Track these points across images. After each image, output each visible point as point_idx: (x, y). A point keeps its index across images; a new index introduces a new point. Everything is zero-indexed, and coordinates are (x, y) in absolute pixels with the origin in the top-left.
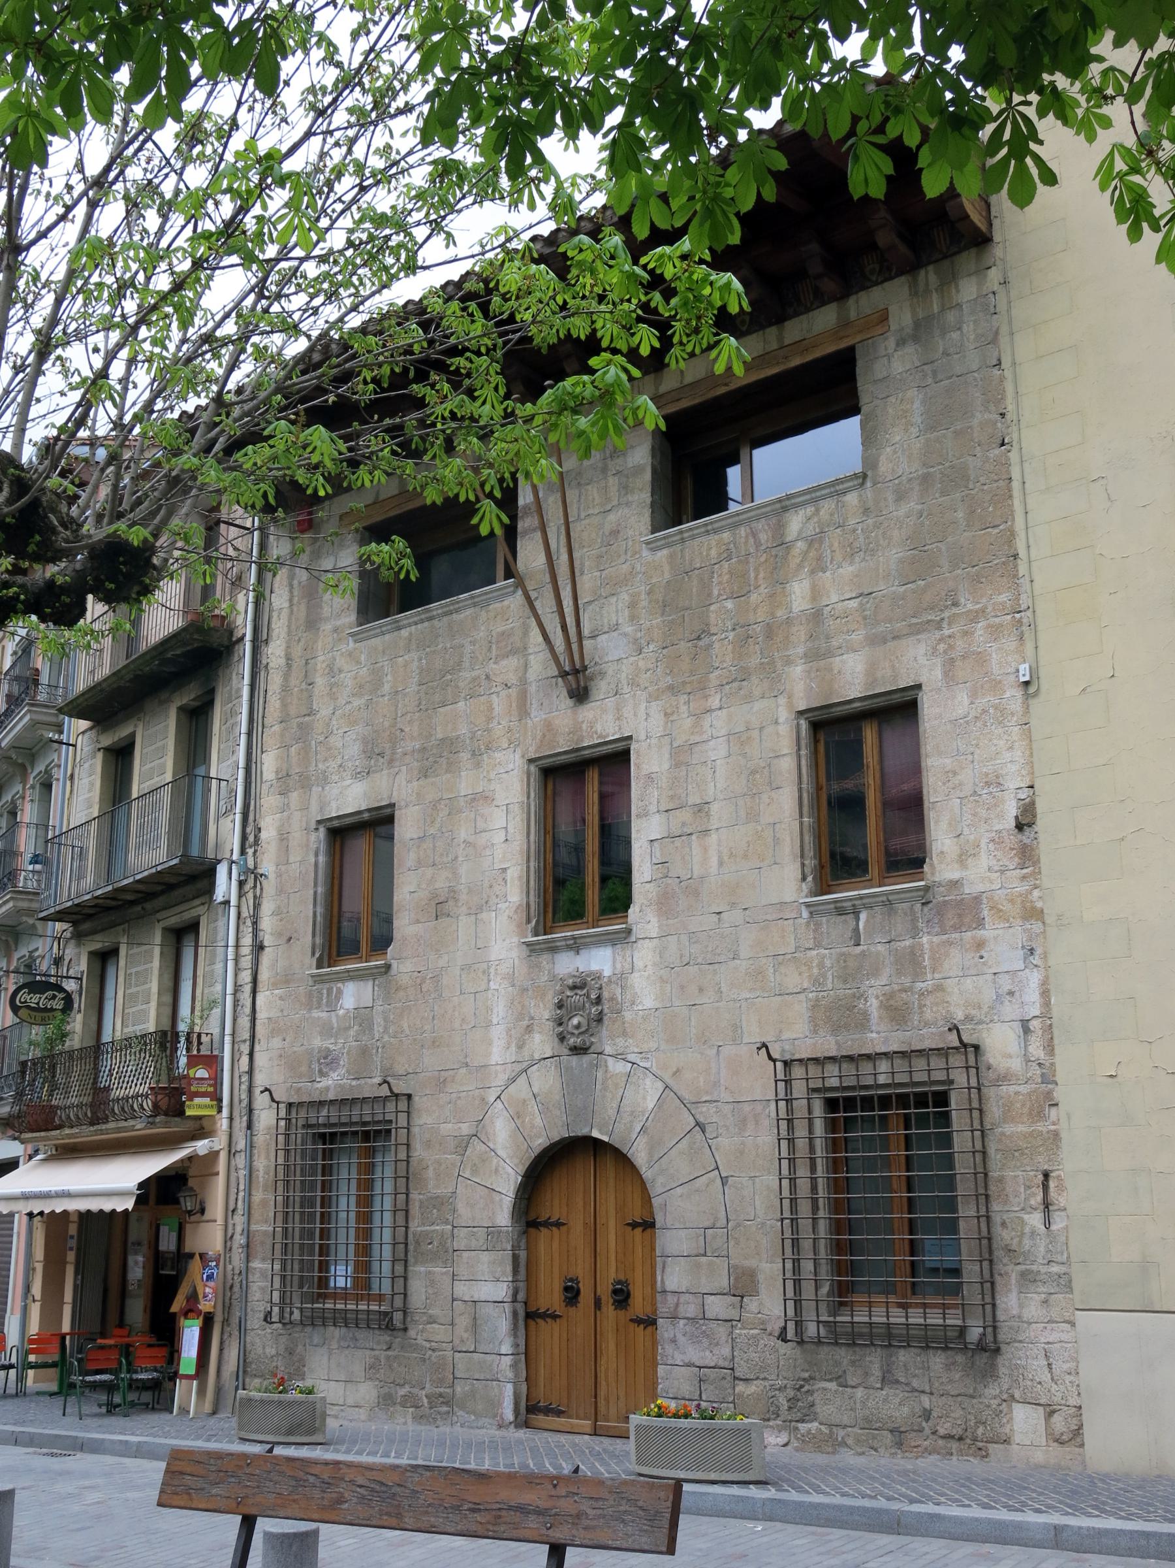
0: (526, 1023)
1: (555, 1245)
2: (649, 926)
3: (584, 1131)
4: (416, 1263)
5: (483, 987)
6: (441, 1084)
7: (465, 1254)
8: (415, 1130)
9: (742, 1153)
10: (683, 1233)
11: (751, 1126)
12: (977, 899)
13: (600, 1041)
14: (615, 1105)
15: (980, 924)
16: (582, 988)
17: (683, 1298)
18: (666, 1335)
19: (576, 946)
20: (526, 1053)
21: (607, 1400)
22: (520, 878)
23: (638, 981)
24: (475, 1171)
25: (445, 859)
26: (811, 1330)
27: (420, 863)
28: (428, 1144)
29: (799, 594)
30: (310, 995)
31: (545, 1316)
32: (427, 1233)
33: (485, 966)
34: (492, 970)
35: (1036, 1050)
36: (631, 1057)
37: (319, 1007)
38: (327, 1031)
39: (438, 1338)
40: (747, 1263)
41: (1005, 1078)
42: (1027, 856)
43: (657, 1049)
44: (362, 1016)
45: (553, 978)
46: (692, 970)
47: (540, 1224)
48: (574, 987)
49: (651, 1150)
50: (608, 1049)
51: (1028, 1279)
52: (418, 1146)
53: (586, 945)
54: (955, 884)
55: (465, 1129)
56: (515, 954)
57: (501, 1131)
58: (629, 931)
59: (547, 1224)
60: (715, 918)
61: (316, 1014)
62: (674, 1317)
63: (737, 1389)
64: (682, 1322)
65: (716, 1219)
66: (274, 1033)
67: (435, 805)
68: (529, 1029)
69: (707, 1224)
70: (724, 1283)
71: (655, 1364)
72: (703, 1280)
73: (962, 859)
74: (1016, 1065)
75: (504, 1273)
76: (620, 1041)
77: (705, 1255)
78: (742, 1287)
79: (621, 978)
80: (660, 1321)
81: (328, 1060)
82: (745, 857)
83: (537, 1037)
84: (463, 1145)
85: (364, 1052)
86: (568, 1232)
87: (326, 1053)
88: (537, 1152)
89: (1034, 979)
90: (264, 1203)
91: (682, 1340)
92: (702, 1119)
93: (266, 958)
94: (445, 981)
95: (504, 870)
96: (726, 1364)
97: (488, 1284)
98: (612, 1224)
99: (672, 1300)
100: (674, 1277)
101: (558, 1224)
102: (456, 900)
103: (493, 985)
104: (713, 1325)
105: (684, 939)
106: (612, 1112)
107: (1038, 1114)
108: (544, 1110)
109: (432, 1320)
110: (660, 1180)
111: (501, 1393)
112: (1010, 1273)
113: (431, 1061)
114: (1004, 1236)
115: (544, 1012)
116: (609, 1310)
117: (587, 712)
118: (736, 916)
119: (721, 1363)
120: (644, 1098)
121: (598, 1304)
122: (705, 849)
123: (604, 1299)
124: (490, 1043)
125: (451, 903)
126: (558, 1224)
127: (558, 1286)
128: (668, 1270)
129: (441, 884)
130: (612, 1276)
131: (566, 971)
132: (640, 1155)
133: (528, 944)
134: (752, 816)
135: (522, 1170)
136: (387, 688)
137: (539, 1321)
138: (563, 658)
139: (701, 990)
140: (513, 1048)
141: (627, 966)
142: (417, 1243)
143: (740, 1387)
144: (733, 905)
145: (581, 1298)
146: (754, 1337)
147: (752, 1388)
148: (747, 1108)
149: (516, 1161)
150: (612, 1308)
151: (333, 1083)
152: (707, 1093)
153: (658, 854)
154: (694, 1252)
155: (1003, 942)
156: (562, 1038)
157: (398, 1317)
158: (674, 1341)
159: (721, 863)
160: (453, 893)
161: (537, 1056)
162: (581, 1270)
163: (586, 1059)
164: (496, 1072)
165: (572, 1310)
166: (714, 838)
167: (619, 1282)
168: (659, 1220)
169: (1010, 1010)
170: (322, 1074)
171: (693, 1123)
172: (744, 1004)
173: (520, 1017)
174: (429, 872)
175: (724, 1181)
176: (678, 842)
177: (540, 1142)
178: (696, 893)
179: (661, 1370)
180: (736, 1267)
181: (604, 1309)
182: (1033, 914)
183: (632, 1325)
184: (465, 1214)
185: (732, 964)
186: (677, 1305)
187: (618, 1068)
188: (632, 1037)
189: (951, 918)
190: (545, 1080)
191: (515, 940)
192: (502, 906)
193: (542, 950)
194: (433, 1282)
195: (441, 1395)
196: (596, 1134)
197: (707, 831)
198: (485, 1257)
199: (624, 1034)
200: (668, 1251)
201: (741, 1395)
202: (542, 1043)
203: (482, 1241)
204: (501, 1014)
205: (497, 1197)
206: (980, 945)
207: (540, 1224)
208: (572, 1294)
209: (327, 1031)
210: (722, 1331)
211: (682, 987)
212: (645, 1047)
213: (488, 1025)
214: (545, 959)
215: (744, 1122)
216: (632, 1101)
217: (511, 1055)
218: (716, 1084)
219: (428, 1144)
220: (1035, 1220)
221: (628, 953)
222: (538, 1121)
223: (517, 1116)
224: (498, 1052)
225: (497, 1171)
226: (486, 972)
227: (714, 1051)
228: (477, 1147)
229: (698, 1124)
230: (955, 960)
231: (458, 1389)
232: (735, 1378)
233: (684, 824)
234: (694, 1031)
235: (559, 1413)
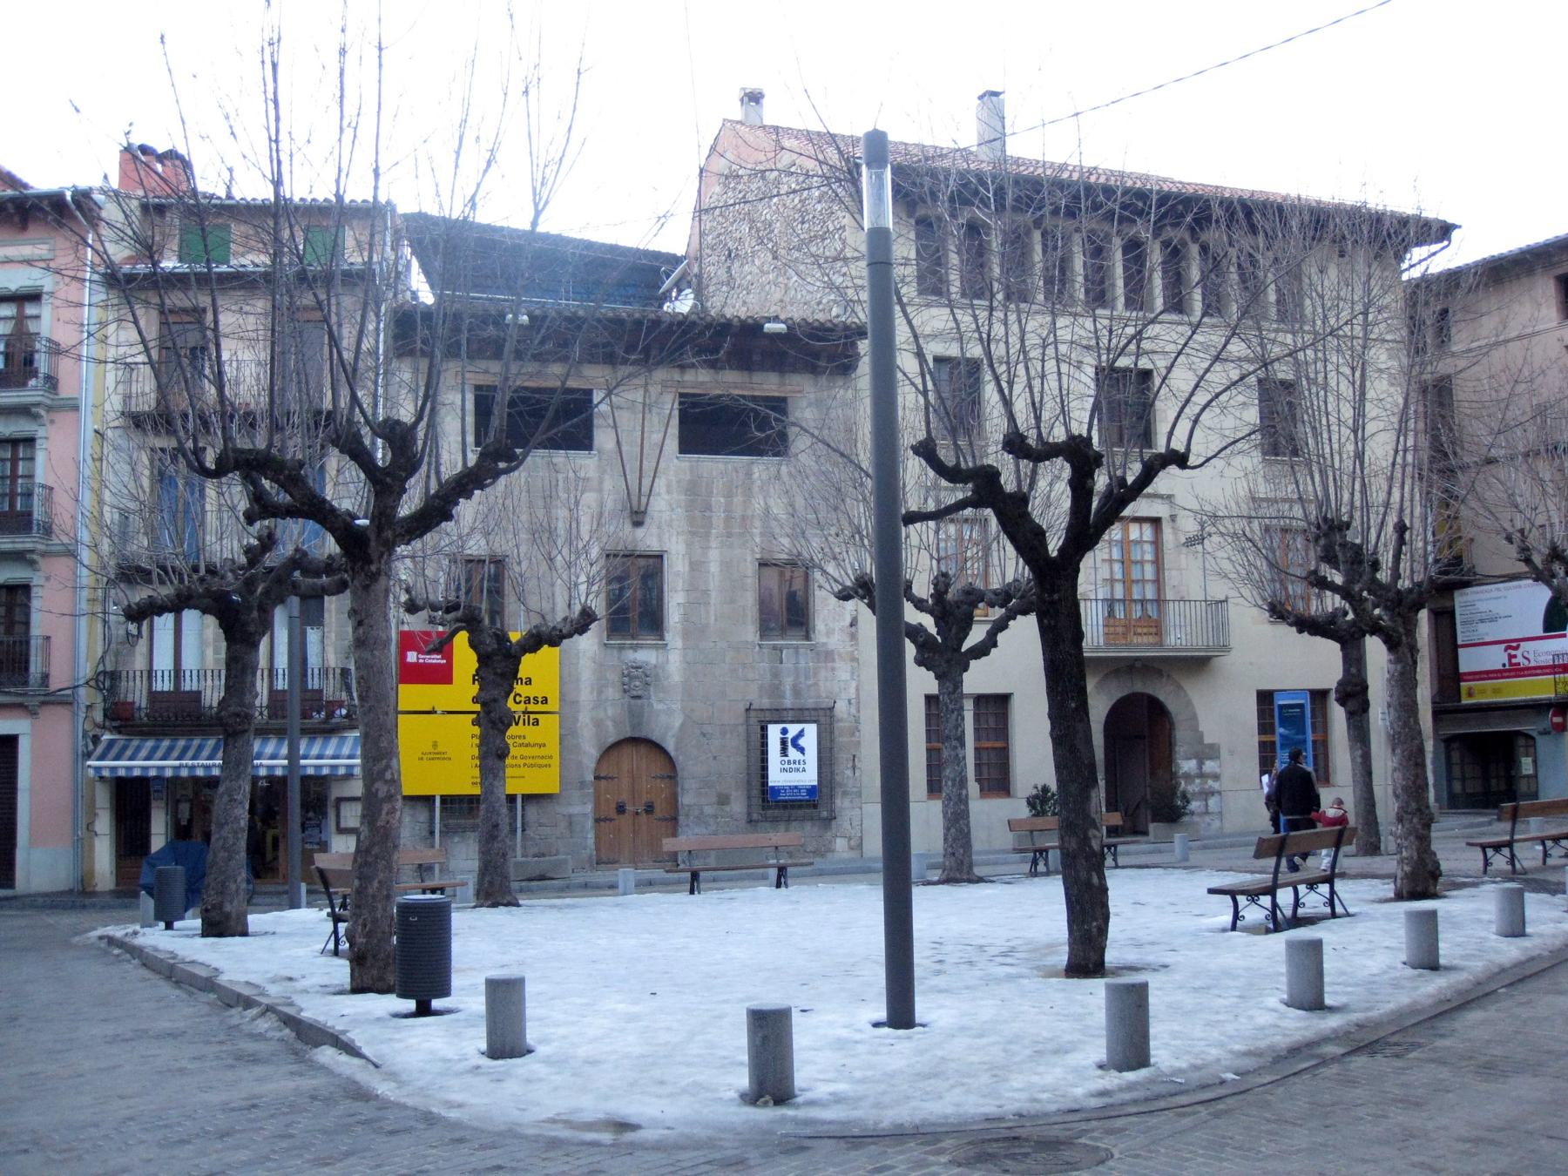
15: (833, 661)
19: (635, 648)
26: (755, 816)
29: (758, 505)
31: (606, 820)
35: (853, 711)
41: (841, 720)
42: (853, 637)
51: (845, 793)
54: (825, 644)
56: (596, 647)
73: (829, 633)
78: (723, 800)
89: (854, 684)
100: (686, 799)
107: (853, 734)
112: (839, 791)
114: (838, 778)
115: (613, 676)
117: (640, 532)
132: (670, 746)
134: (732, 601)
138: (635, 503)
156: (625, 691)
177: (611, 740)
182: (854, 660)
202: (612, 693)
206: (833, 669)
208: (621, 809)
210: (711, 821)
216: (667, 720)
220: (849, 773)
222: (611, 728)
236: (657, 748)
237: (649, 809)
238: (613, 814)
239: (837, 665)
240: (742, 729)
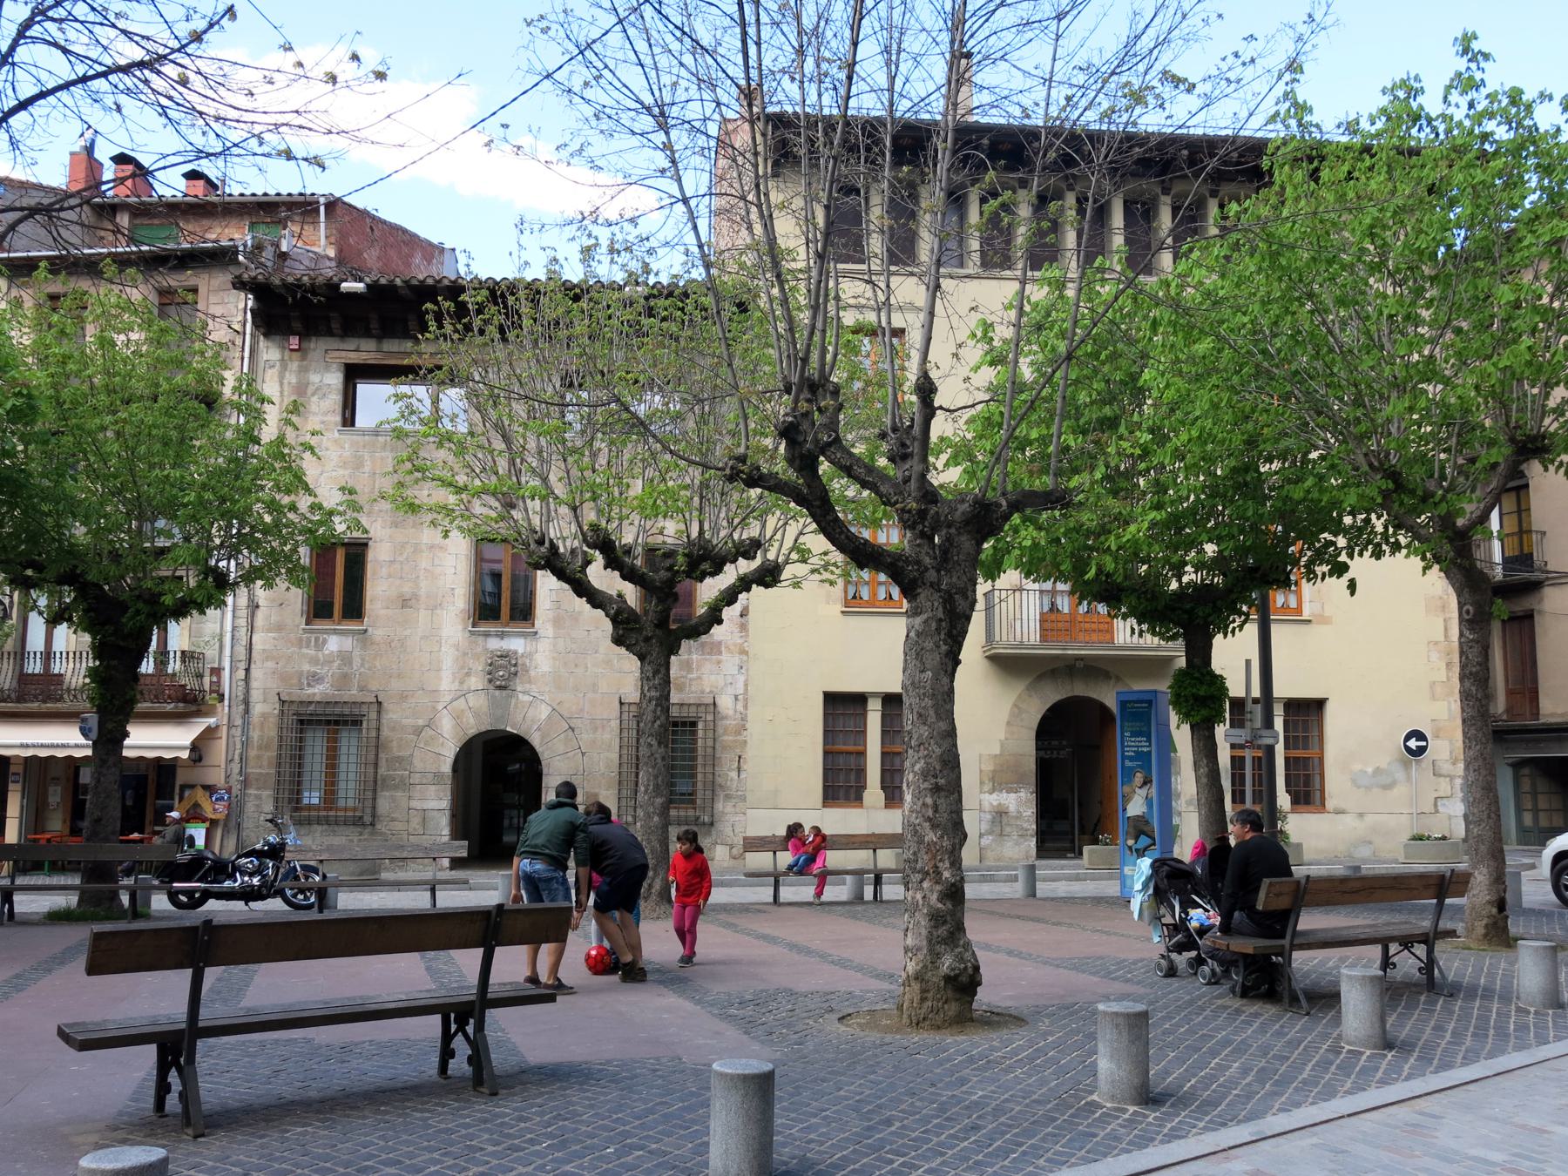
6: (403, 697)
8: (384, 721)
12: (720, 643)
15: (720, 653)
19: (502, 636)
23: (539, 658)
27: (390, 576)
28: (393, 729)
30: (301, 640)
35: (740, 707)
37: (308, 647)
38: (314, 661)
41: (726, 718)
44: (345, 658)
51: (728, 797)
55: (421, 722)
57: (446, 725)
61: (305, 651)
66: (267, 659)
67: (403, 545)
68: (468, 674)
74: (731, 712)
79: (530, 655)
81: (315, 679)
83: (473, 679)
84: (418, 731)
85: (345, 676)
87: (314, 675)
89: (742, 679)
90: (258, 757)
93: (260, 614)
97: (436, 802)
106: (519, 719)
107: (738, 733)
108: (477, 715)
109: (393, 820)
113: (396, 685)
114: (719, 780)
115: (479, 666)
124: (440, 679)
129: (407, 589)
132: (535, 741)
136: (367, 469)
142: (384, 780)
151: (318, 691)
155: (730, 662)
156: (490, 681)
157: (368, 819)
160: (416, 596)
169: (730, 690)
170: (309, 685)
173: (462, 668)
174: (398, 582)
177: (472, 732)
178: (576, 620)
182: (744, 652)
184: (418, 765)
187: (526, 698)
189: (707, 649)
190: (479, 701)
199: (530, 682)
202: (476, 682)
209: (314, 661)
214: (480, 639)
215: (595, 729)
216: (531, 716)
217: (456, 686)
218: (582, 710)
219: (393, 729)
220: (734, 774)
222: (472, 721)
223: (457, 718)
224: (446, 683)
228: (428, 732)
230: (707, 667)
239: (723, 657)
240: (615, 724)
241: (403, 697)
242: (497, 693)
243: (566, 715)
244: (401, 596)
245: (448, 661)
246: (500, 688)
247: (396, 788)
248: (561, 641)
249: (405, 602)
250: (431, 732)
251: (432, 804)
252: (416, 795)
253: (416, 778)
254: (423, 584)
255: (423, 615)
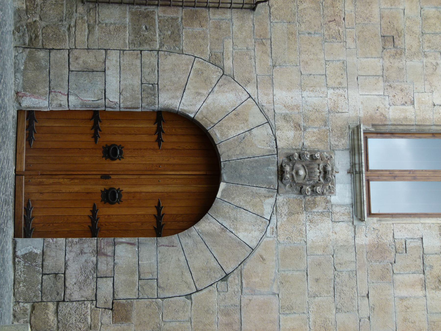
0: (302, 124)
1: (145, 138)
2: (364, 237)
3: (224, 177)
4: (132, 14)
5: (330, 83)
6: (262, 40)
7: (138, 62)
8: (228, 14)
9: (207, 312)
10: (154, 260)
11: (223, 319)
13: (287, 192)
14: (242, 204)
16: (325, 178)
17: (110, 259)
18: (86, 246)
20: (280, 123)
21: (40, 184)
22: (406, 118)
23: (326, 225)
24: (199, 73)
25: (426, 44)
27: (425, 18)
28: (218, 27)
31: (96, 128)
32: (153, 25)
33: (345, 85)
34: (341, 91)
36: (274, 217)
39: (78, 36)
40: (134, 314)
43: (279, 243)
45: (333, 150)
46: (331, 273)
47: (159, 125)
48: (325, 172)
49: (210, 235)
50: (280, 199)
52: (217, 17)
53: (354, 182)
55: (228, 64)
56: (352, 113)
57: (225, 98)
58: (362, 219)
59: (159, 131)
60: (365, 294)
62: (98, 252)
63: (50, 304)
64: (94, 259)
65: (163, 289)
68: (297, 127)
69: (160, 281)
70: (121, 295)
71: (66, 235)
72: (123, 277)
75: (125, 99)
76: (285, 210)
77: (140, 279)
79: (329, 212)
80: (94, 240)
82: (405, 320)
83: (291, 134)
84: (216, 61)
86: (154, 149)
88: (211, 132)
91: (83, 259)
92: (230, 279)
94: (336, 45)
95: (413, 103)
96: (67, 296)
97: (117, 86)
98: (159, 189)
99: (109, 250)
100: (125, 252)
101: (159, 141)
102: (394, 56)
103: (331, 91)
104: (93, 285)
105: (352, 267)
108: (241, 139)
110: (190, 242)
111: (40, 96)
113: (278, 30)
115: (310, 141)
116: (100, 188)
118: (365, 312)
119: (68, 291)
120: (246, 230)
121: (106, 177)
122: (413, 286)
123: (108, 182)
124: (289, 89)
125: (393, 51)
126: (159, 141)
127: (117, 139)
128: (129, 247)
129: (409, 42)
130: (125, 189)
131: (337, 162)
132: (206, 225)
133: (358, 127)
135: (199, 117)
137: (90, 124)
139: (317, 280)
140: (285, 111)
141: (336, 217)
142: (147, 16)
143: (52, 307)
144: (372, 309)
145: (108, 161)
146: (86, 319)
147: (52, 317)
148: (237, 317)
149: (205, 112)
150: (102, 188)
152: (248, 284)
153: (412, 245)
154: (141, 270)
156: (290, 157)
158: (82, 252)
159: (402, 299)
160: (399, 53)
161: (278, 133)
162: (128, 161)
163: (274, 178)
164: (267, 95)
165: (100, 153)
166: (421, 293)
167: (120, 196)
168: (164, 240)
171: (228, 271)
172: (305, 316)
173: (306, 118)
174: (417, 29)
175: (188, 296)
176: (419, 262)
177: (217, 135)
178: (383, 278)
179: (61, 241)
180: (131, 305)
181: (102, 181)
183: (90, 205)
184: (169, 61)
185: (333, 306)
186: (106, 255)
187: (267, 210)
188: (288, 221)
190: (261, 142)
191: (361, 114)
192: (387, 103)
193: (353, 140)
194: (117, 30)
195: (37, 36)
196: (222, 186)
197: (424, 287)
198: (137, 82)
199: (291, 214)
200: (142, 248)
201: (47, 307)
203: (148, 78)
204: (309, 99)
205: (179, 94)
207: (159, 125)
208: (112, 152)
210: (88, 292)
211: (320, 264)
212: (280, 232)
213: (302, 87)
214: (345, 142)
215: (227, 314)
217: (280, 110)
218: (253, 292)
219: (218, 27)
221: (346, 218)
222: (232, 133)
223: (236, 113)
224: (283, 97)
225: (198, 94)
226: (340, 86)
227: (276, 291)
229: (227, 275)
231: (42, 54)
232: (58, 302)
233: (431, 267)
234: (290, 274)
235: (29, 139)
236: (203, 203)
237: (111, 196)
238: (107, 139)
241: (262, 40)
242: (274, 168)
243: (246, 267)
244: (400, 34)
245: (314, 99)
246: (281, 173)
247: (136, 31)
248: (351, 257)
249: (390, 40)
250: (215, 77)
251: (113, 81)
252: (127, 59)
253: (149, 59)
254: (416, 63)
255: (374, 63)
